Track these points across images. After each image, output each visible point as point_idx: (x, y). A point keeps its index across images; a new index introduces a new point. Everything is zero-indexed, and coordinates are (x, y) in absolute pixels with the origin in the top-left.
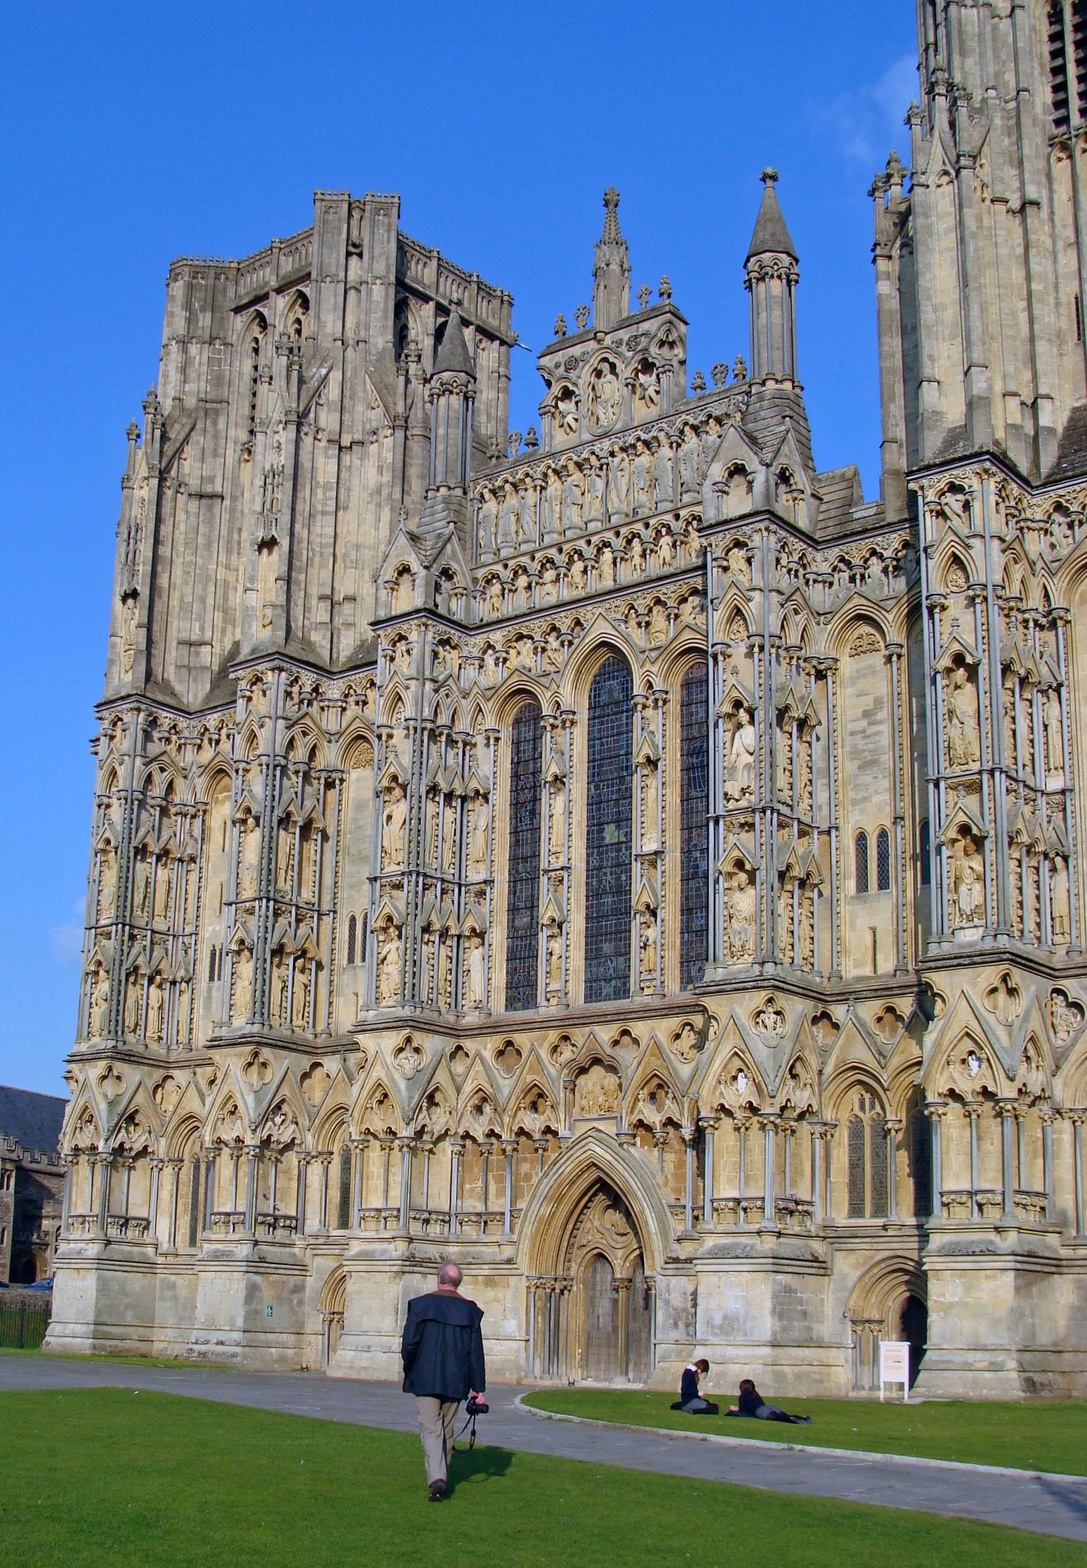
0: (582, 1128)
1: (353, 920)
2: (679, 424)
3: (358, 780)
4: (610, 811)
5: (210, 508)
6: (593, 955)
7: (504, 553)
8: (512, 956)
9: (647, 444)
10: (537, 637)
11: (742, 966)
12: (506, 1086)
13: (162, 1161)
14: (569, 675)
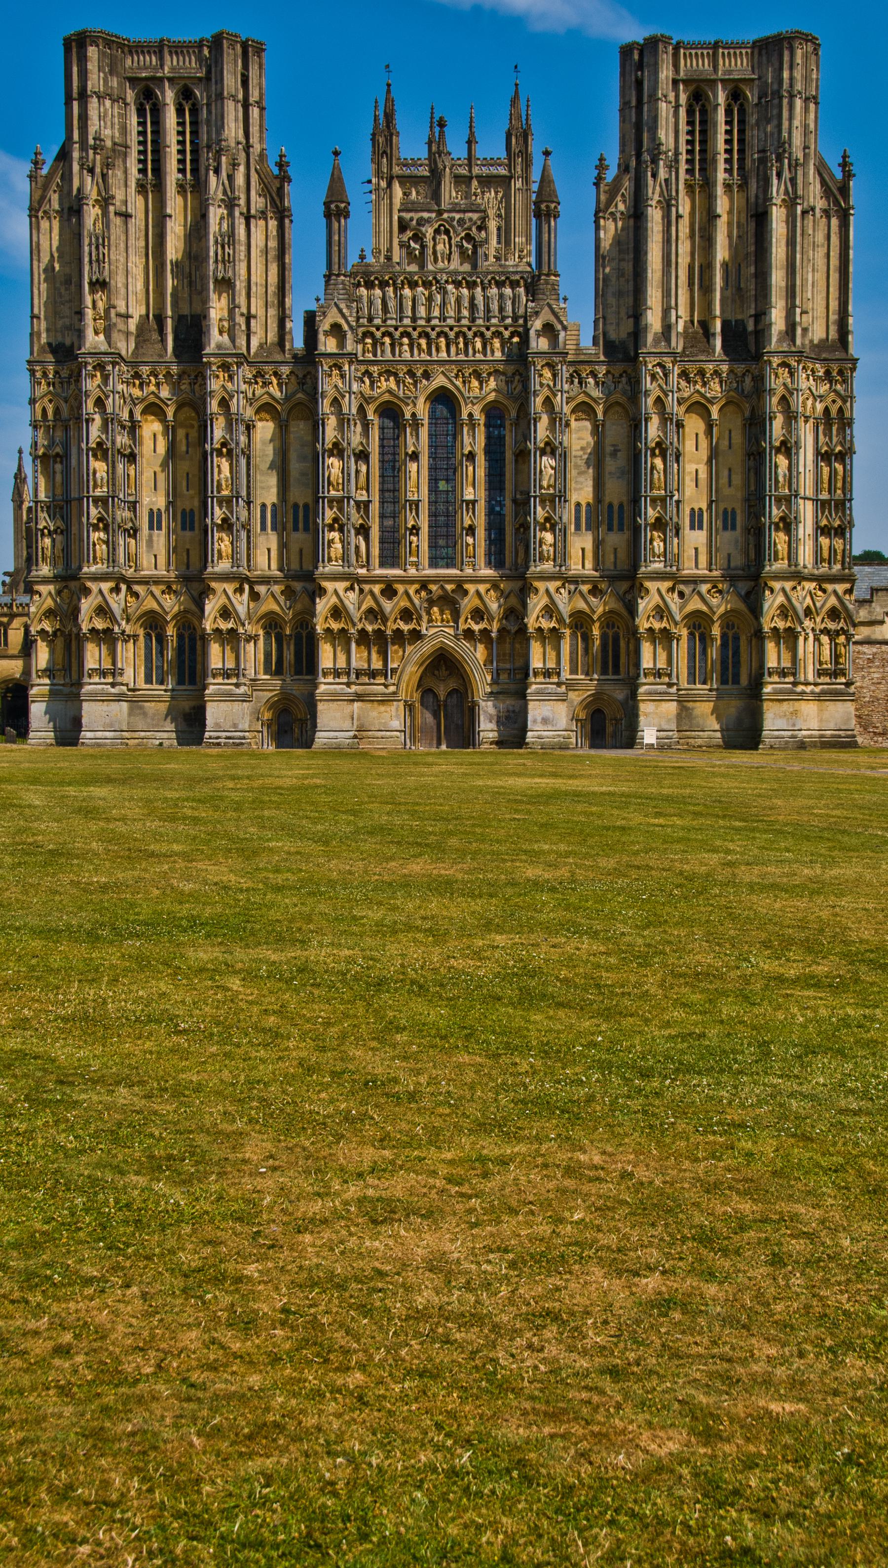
0: (432, 631)
1: (264, 506)
2: (489, 277)
3: (263, 428)
4: (441, 474)
5: (126, 224)
6: (433, 546)
7: (378, 321)
8: (382, 541)
9: (467, 282)
10: (401, 375)
11: (548, 566)
12: (388, 606)
13: (128, 636)
14: (421, 400)
